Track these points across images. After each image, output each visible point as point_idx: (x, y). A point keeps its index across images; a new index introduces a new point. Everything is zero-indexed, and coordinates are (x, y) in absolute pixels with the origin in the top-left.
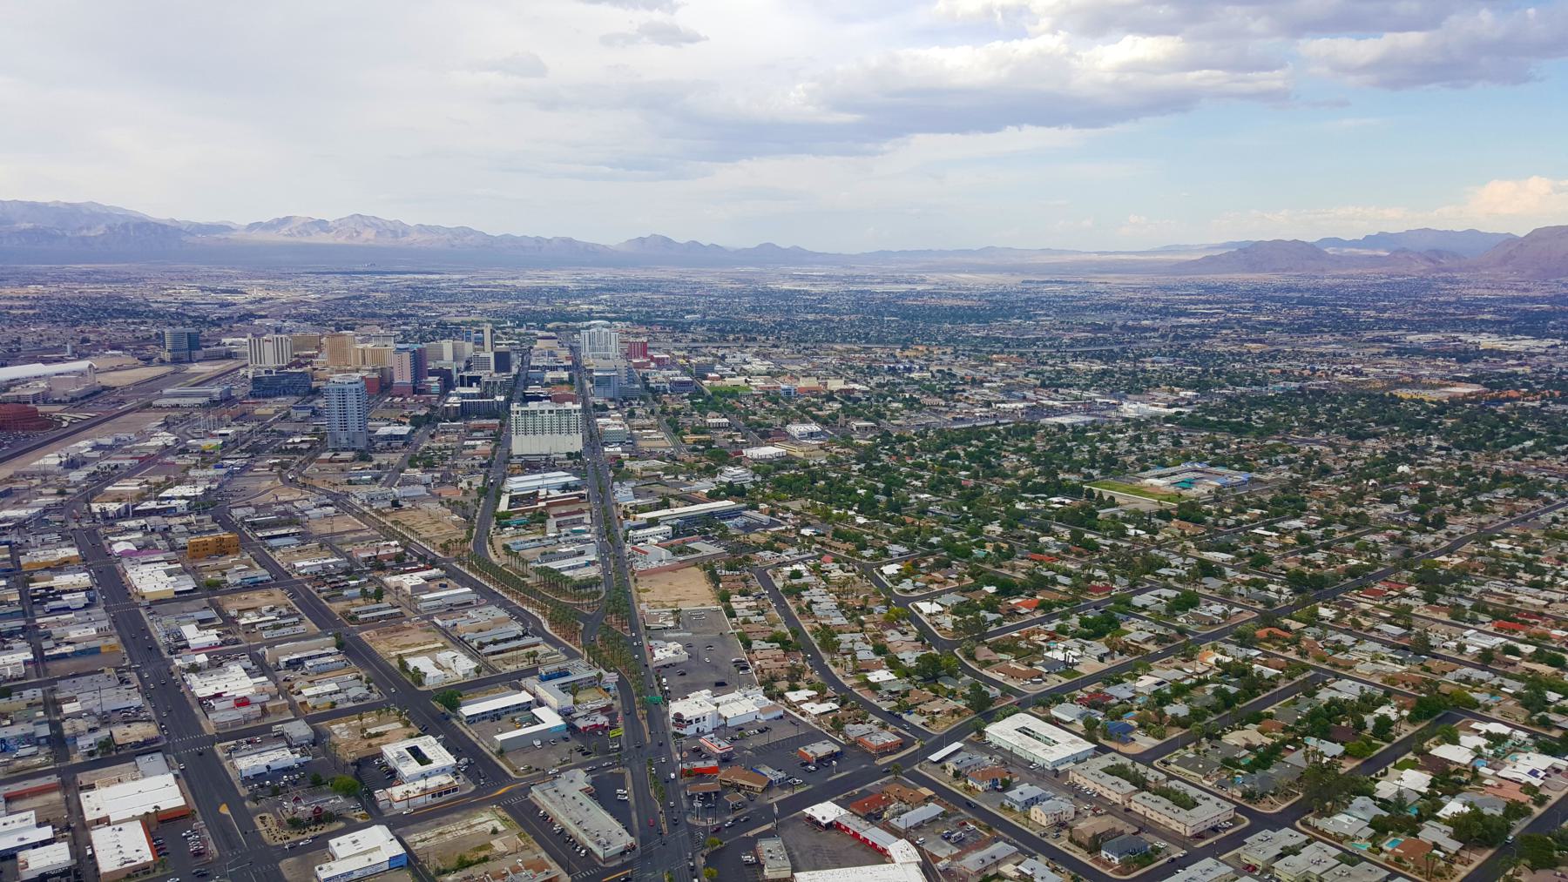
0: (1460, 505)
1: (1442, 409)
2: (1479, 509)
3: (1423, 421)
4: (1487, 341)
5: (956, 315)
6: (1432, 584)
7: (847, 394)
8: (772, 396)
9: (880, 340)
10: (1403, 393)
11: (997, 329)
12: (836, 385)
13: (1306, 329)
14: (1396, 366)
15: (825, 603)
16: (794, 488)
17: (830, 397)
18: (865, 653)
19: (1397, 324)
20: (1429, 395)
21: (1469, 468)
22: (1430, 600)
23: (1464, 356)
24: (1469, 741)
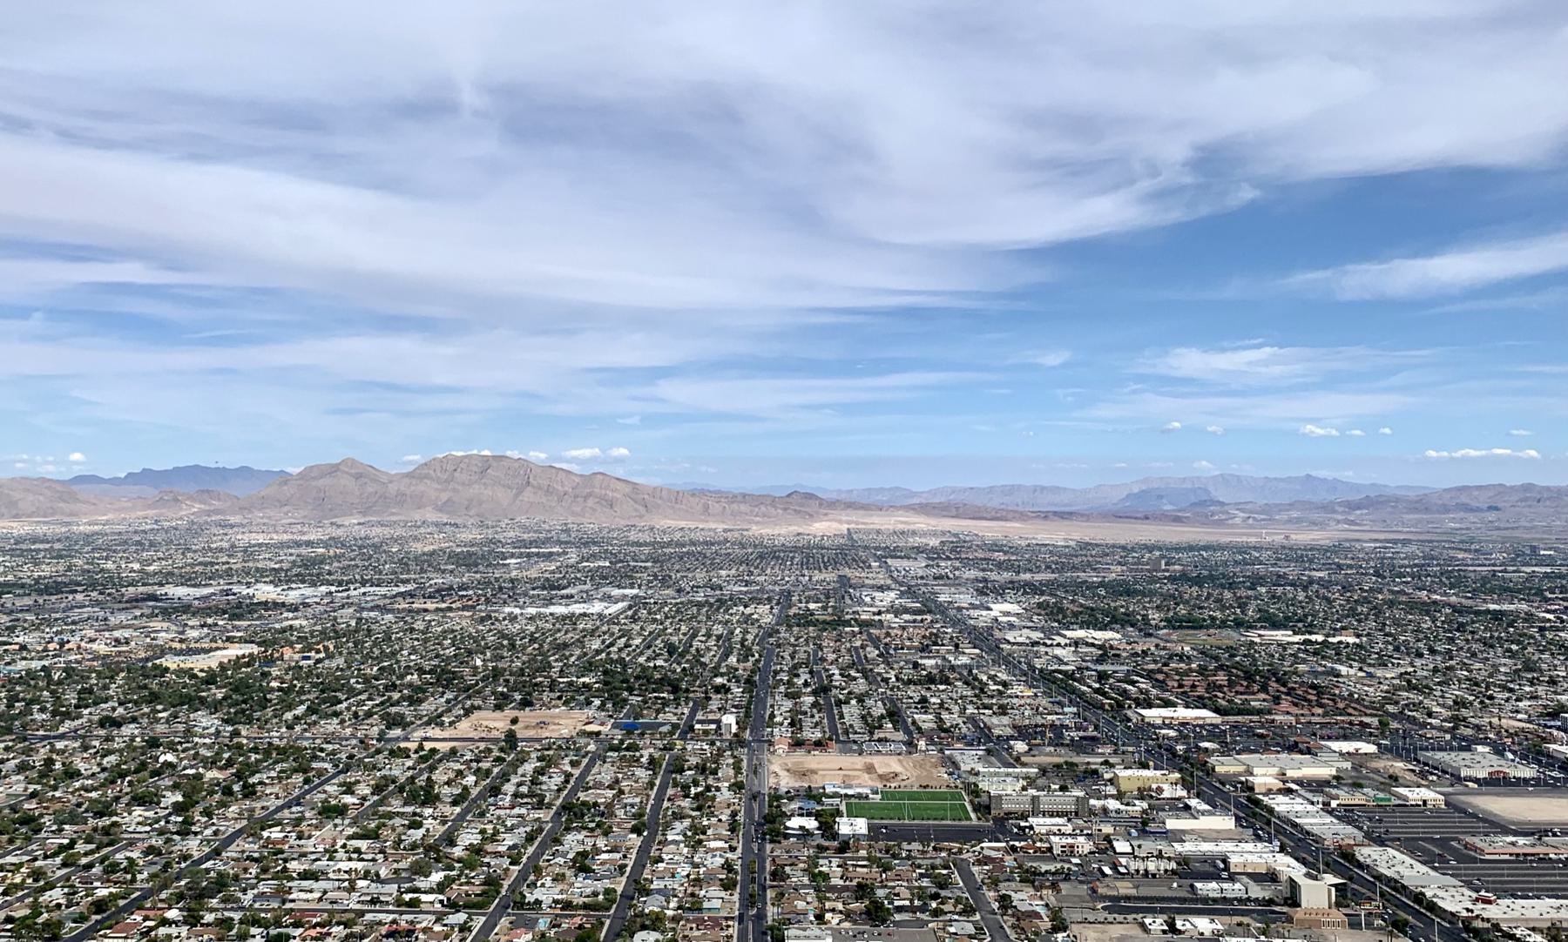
0: (228, 791)
1: (211, 679)
2: (250, 792)
3: (189, 694)
10: (171, 662)
14: (165, 632)
19: (167, 577)
20: (199, 664)
21: (239, 746)
23: (240, 609)
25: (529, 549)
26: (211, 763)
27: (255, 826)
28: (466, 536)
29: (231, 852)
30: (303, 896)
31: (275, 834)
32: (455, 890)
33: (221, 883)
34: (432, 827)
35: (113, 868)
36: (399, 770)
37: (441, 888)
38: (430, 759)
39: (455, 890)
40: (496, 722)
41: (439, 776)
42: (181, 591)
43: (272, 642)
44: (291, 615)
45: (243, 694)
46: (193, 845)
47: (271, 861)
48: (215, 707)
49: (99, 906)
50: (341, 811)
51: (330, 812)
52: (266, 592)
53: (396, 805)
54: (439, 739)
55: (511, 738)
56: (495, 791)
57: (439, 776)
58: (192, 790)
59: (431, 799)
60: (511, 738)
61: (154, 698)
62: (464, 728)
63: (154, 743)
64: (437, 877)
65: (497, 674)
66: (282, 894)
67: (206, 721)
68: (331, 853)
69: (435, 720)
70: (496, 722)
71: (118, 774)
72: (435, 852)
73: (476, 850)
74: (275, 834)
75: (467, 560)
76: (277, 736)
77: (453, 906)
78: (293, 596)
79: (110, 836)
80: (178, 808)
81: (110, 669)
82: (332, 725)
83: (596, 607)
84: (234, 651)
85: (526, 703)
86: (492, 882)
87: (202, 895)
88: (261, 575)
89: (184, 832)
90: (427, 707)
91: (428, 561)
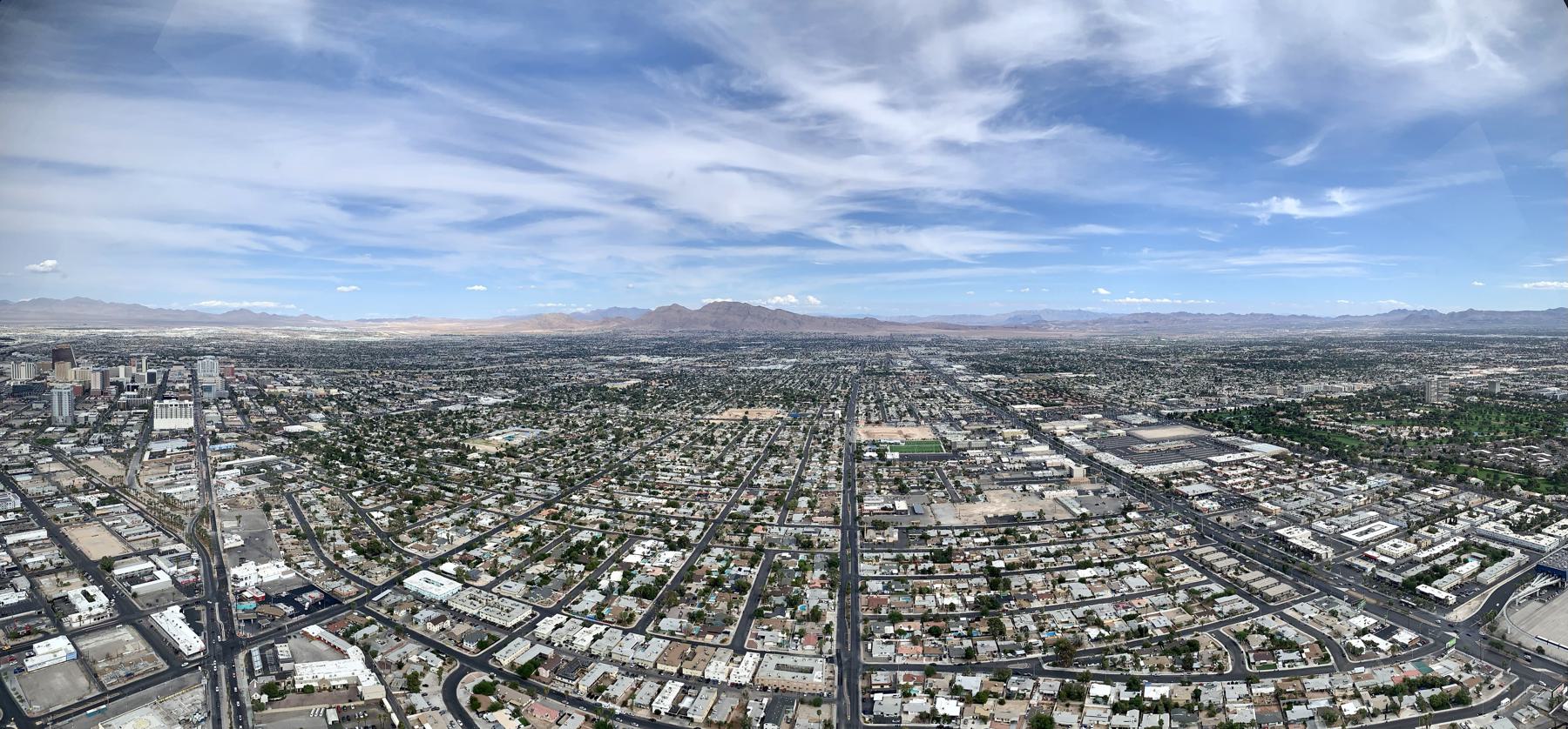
1: (624, 392)
2: (641, 436)
3: (617, 398)
4: (644, 358)
5: (397, 354)
6: (622, 474)
7: (339, 397)
8: (303, 398)
9: (359, 367)
10: (609, 385)
11: (419, 359)
12: (334, 392)
13: (567, 356)
14: (607, 373)
15: (323, 512)
16: (310, 448)
17: (331, 398)
18: (340, 542)
20: (620, 386)
22: (621, 483)
24: (639, 550)
25: (750, 342)
26: (626, 424)
27: (643, 450)
28: (724, 336)
29: (635, 459)
30: (663, 478)
31: (651, 453)
32: (724, 480)
33: (631, 470)
34: (715, 454)
35: (591, 462)
36: (700, 431)
37: (718, 478)
38: (712, 427)
39: (724, 480)
40: (740, 413)
41: (716, 434)
42: (612, 358)
43: (647, 378)
44: (654, 370)
45: (636, 398)
46: (620, 455)
47: (650, 464)
48: (626, 403)
49: (587, 475)
50: (677, 446)
51: (673, 446)
52: (644, 358)
53: (699, 444)
54: (716, 419)
55: (745, 420)
56: (739, 440)
57: (716, 434)
58: (619, 435)
59: (713, 443)
60: (745, 420)
61: (604, 399)
62: (726, 415)
63: (604, 416)
64: (717, 473)
65: (738, 394)
66: (655, 476)
67: (622, 408)
68: (674, 462)
69: (714, 411)
70: (740, 413)
71: (592, 427)
72: (715, 464)
73: (733, 463)
74: (651, 453)
75: (724, 347)
76: (651, 415)
77: (724, 485)
78: (655, 360)
79: (590, 449)
80: (614, 441)
81: (588, 388)
82: (673, 412)
83: (780, 367)
84: (633, 382)
85: (751, 406)
86: (740, 477)
87: (624, 474)
88: (642, 352)
89: (617, 450)
90: (711, 406)
91: (709, 347)
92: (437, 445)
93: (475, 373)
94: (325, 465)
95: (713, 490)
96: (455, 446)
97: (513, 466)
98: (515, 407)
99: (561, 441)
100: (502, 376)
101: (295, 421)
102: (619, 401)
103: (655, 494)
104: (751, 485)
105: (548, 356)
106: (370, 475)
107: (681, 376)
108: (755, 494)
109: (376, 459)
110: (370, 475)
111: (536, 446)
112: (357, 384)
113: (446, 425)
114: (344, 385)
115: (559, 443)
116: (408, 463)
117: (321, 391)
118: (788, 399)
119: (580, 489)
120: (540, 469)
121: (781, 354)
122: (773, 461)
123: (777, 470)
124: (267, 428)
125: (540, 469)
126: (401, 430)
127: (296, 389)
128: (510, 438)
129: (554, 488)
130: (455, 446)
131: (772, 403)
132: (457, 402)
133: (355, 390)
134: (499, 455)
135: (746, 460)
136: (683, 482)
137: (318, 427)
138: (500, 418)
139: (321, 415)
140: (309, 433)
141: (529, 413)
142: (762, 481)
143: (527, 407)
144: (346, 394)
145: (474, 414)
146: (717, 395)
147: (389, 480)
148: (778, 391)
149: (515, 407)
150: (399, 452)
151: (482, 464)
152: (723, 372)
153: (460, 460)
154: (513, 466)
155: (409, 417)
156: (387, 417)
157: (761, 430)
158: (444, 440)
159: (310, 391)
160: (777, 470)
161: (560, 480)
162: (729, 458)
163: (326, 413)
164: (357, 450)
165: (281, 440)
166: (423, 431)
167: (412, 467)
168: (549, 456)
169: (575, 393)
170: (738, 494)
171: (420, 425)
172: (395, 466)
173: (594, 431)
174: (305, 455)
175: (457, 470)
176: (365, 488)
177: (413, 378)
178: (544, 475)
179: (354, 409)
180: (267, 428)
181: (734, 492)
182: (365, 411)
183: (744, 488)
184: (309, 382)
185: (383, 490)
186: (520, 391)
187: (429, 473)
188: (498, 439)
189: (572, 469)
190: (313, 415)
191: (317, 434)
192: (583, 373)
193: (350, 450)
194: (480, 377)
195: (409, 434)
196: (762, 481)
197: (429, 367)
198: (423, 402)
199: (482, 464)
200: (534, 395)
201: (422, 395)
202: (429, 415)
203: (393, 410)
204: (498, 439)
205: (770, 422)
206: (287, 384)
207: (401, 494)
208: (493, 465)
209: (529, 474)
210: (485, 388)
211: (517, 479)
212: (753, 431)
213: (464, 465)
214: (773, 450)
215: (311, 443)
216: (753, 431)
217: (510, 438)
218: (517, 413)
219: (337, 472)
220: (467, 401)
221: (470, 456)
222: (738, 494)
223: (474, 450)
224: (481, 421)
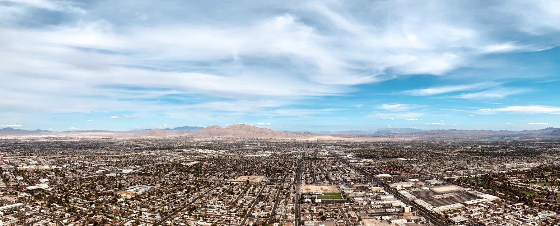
1: (191, 167)
2: (199, 190)
3: (187, 170)
4: (200, 151)
8: (37, 171)
10: (184, 164)
14: (182, 158)
20: (189, 164)
25: (251, 143)
26: (192, 184)
27: (201, 197)
29: (196, 202)
30: (210, 212)
31: (204, 199)
33: (195, 208)
35: (176, 203)
36: (227, 187)
37: (235, 212)
38: (232, 185)
40: (245, 178)
41: (234, 189)
42: (185, 150)
43: (202, 160)
44: (205, 156)
45: (197, 170)
46: (189, 200)
47: (203, 204)
48: (192, 173)
50: (216, 195)
51: (214, 195)
52: (200, 151)
53: (226, 194)
55: (248, 182)
56: (245, 192)
57: (234, 189)
58: (189, 189)
59: (233, 193)
60: (248, 182)
61: (181, 171)
62: (239, 179)
63: (181, 179)
64: (234, 209)
65: (245, 168)
66: (206, 211)
67: (191, 176)
68: (215, 203)
69: (233, 177)
70: (245, 178)
71: (175, 185)
72: (234, 204)
73: (242, 204)
74: (204, 199)
75: (238, 145)
76: (204, 179)
77: (238, 216)
78: (206, 152)
79: (175, 197)
80: (186, 192)
81: (173, 165)
82: (214, 178)
83: (264, 155)
84: (195, 162)
85: (251, 175)
87: (191, 210)
88: (199, 147)
89: (188, 197)
91: (231, 145)
92: (104, 194)
93: (120, 158)
94: (49, 206)
95: (233, 218)
96: (112, 194)
97: (139, 205)
98: (139, 174)
99: (161, 192)
100: (133, 159)
101: (32, 184)
102: (189, 172)
103: (206, 220)
104: (251, 216)
105: (154, 149)
106: (72, 211)
107: (217, 160)
108: (253, 221)
109: (75, 201)
110: (72, 211)
111: (149, 195)
112: (66, 163)
113: (109, 183)
114: (59, 163)
115: (160, 193)
116: (91, 204)
117: (47, 167)
118: (268, 171)
119: (170, 217)
120: (151, 207)
121: (265, 149)
122: (261, 204)
123: (263, 208)
124: (18, 188)
125: (151, 207)
126: (88, 186)
127: (33, 167)
128: (137, 190)
129: (158, 217)
130: (112, 194)
131: (260, 174)
132: (112, 172)
133: (65, 166)
134: (132, 199)
135: (248, 203)
136: (219, 213)
137: (45, 186)
138: (132, 180)
139: (47, 180)
140: (39, 189)
141: (146, 177)
142: (255, 214)
143: (145, 175)
144: (60, 168)
145: (120, 178)
146: (235, 169)
147: (82, 213)
148: (263, 167)
149: (139, 174)
150: (87, 198)
151: (124, 204)
152: (238, 157)
153: (114, 202)
154: (139, 205)
155: (92, 179)
156: (80, 179)
157: (255, 187)
158: (108, 191)
159: (41, 167)
160: (263, 208)
161: (161, 213)
162: (240, 202)
163: (50, 178)
164: (65, 197)
165: (25, 194)
166: (98, 187)
167: (93, 206)
168: (155, 200)
169: (168, 167)
170: (245, 221)
171: (97, 184)
172: (85, 205)
173: (177, 187)
174: (37, 202)
175: (114, 207)
176: (69, 217)
177: (94, 159)
178: (153, 210)
179: (64, 176)
180: (18, 188)
181: (243, 219)
182: (69, 176)
183: (247, 217)
184: (40, 163)
185: (78, 218)
186: (141, 166)
187: (101, 209)
188: (131, 192)
189: (166, 207)
190: (42, 180)
191: (43, 190)
192: (171, 157)
193: (62, 197)
194: (123, 159)
195: (92, 188)
196: (255, 214)
197: (101, 154)
198: (98, 171)
199: (124, 204)
200: (148, 168)
201: (98, 168)
202: (101, 178)
203: (84, 176)
204: (131, 192)
205: (260, 183)
206: (30, 165)
207: (87, 220)
208: (129, 204)
209: (146, 209)
210: (126, 164)
211: (141, 212)
212: (252, 188)
213: (116, 205)
214: (261, 198)
215: (40, 195)
216: (252, 188)
217: (137, 190)
218: (140, 177)
219: (55, 210)
220: (117, 172)
221: (119, 200)
222: (245, 221)
223: (121, 197)
224: (123, 182)
